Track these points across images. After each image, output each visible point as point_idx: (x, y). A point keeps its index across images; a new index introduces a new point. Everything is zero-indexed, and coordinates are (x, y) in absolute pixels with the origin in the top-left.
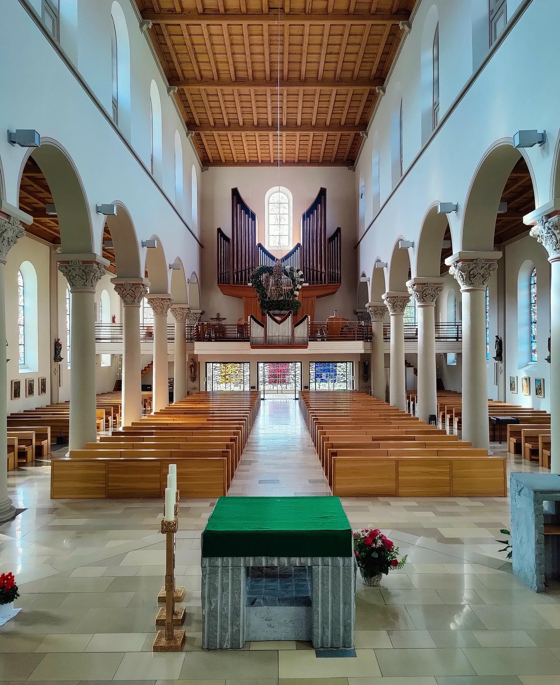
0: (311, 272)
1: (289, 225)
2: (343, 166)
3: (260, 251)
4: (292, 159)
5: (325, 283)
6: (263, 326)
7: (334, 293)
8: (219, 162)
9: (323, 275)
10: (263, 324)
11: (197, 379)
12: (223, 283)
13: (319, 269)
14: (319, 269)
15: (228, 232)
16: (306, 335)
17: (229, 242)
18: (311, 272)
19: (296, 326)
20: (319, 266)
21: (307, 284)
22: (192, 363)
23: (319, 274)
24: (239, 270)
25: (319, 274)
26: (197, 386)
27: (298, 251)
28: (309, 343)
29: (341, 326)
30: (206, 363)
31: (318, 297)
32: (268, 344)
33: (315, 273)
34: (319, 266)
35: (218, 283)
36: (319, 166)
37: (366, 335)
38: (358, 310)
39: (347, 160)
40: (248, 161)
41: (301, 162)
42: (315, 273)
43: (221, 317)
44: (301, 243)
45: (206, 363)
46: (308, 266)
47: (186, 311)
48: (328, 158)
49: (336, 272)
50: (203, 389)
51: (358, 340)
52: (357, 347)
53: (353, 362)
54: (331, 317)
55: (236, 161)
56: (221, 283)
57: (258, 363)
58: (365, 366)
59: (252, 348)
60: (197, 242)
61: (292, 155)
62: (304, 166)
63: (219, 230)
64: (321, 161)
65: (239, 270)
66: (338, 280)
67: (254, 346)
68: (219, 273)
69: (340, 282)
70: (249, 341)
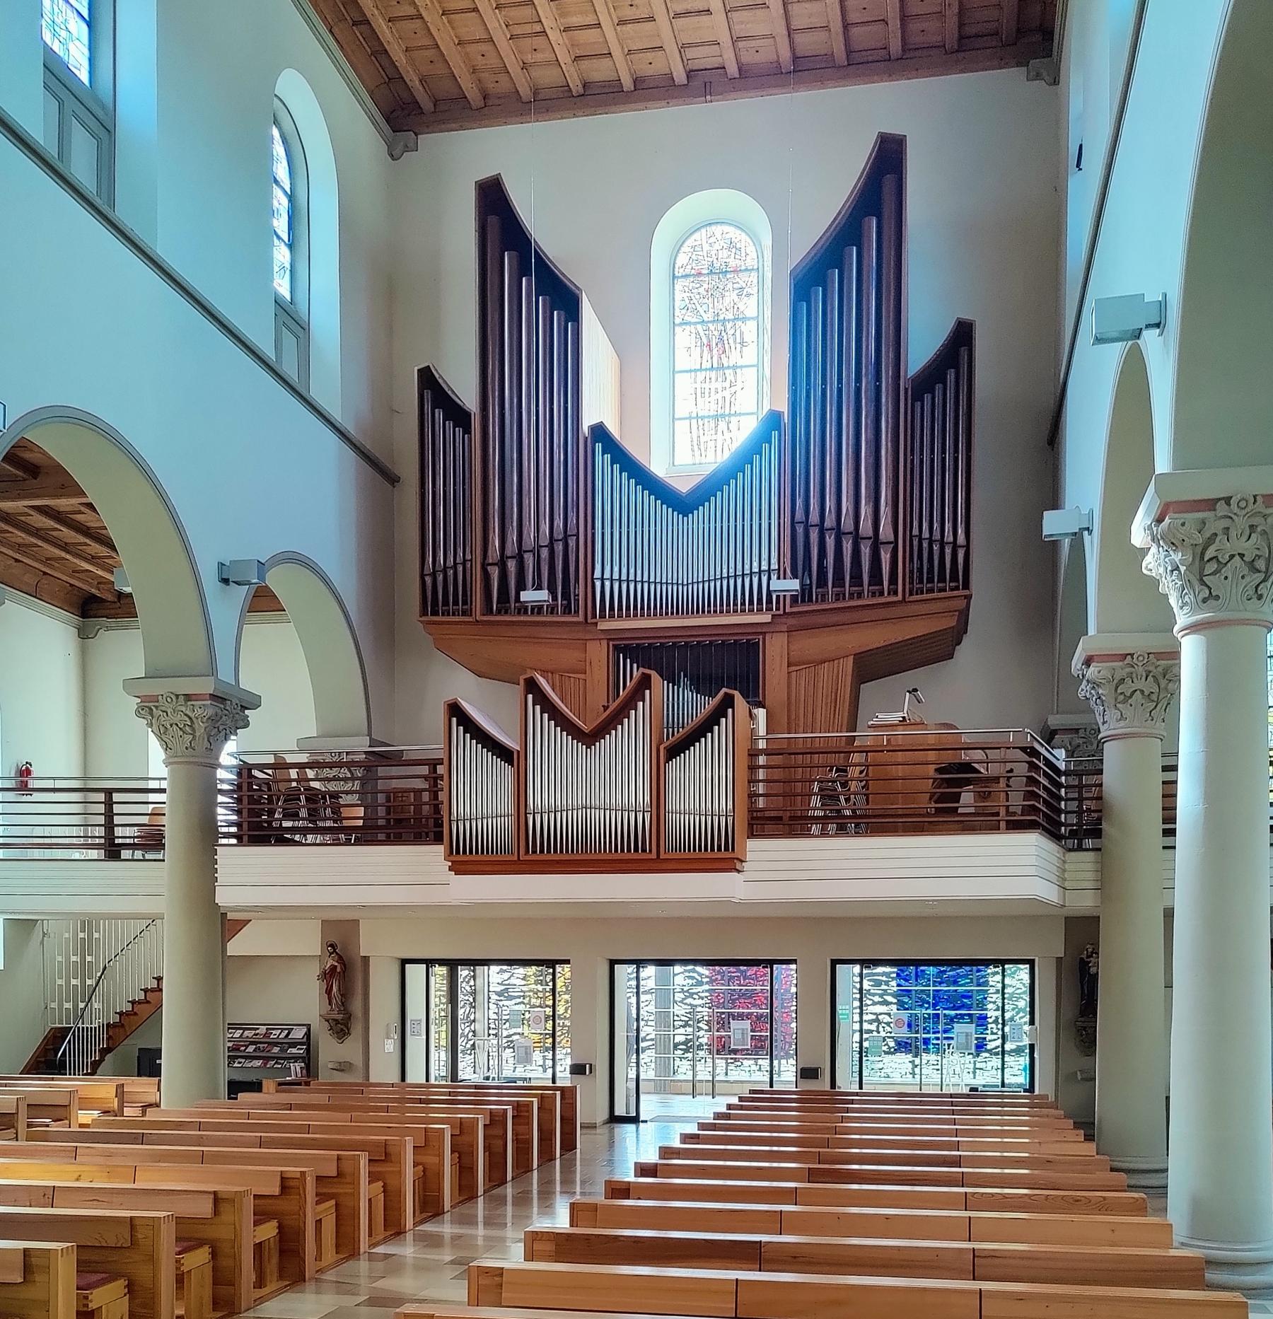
0: (830, 542)
1: (758, 366)
3: (602, 460)
6: (504, 753)
9: (885, 557)
11: (357, 1029)
13: (866, 527)
14: (866, 527)
16: (723, 803)
17: (467, 430)
18: (830, 542)
19: (676, 750)
20: (865, 510)
22: (330, 962)
23: (866, 551)
24: (511, 548)
25: (866, 551)
26: (358, 1061)
32: (534, 852)
33: (847, 546)
34: (865, 510)
37: (1068, 809)
38: (1054, 721)
42: (847, 546)
45: (404, 962)
46: (814, 517)
47: (203, 710)
49: (949, 537)
50: (383, 1070)
51: (1016, 826)
57: (613, 963)
59: (459, 868)
60: (332, 437)
63: (428, 379)
65: (511, 548)
66: (954, 577)
67: (468, 860)
69: (966, 585)
70: (438, 839)
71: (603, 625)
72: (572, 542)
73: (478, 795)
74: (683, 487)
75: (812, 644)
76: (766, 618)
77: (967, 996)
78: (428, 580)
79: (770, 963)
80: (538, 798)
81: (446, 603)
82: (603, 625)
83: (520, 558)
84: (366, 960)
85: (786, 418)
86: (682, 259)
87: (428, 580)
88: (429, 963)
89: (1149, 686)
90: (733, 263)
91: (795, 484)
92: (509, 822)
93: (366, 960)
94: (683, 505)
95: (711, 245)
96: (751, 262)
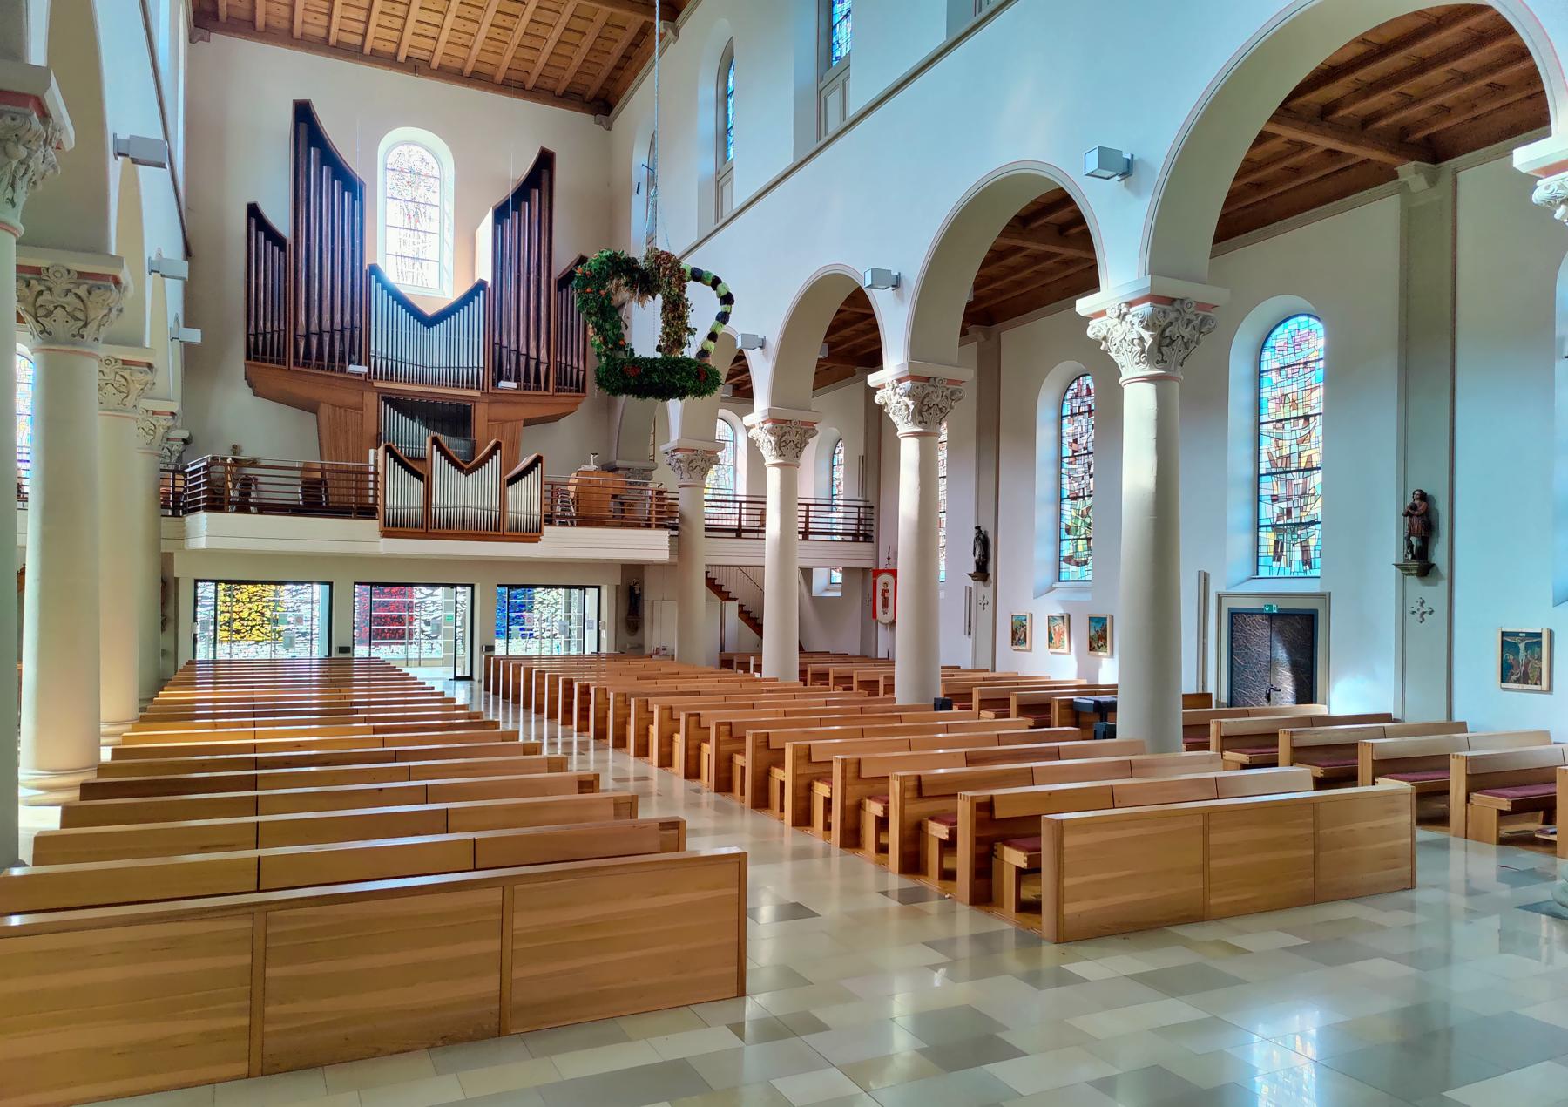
2: (583, 111)
4: (457, 64)
5: (546, 388)
7: (555, 418)
8: (246, 26)
9: (543, 368)
10: (414, 467)
11: (170, 627)
12: (264, 361)
13: (533, 353)
14: (533, 353)
15: (281, 221)
20: (533, 344)
21: (513, 385)
24: (314, 327)
25: (532, 363)
27: (479, 300)
28: (546, 529)
29: (611, 491)
30: (197, 581)
31: (528, 423)
32: (430, 526)
33: (523, 359)
34: (533, 344)
35: (248, 358)
36: (525, 97)
39: (596, 99)
40: (332, 40)
41: (477, 78)
42: (523, 359)
43: (247, 454)
44: (488, 278)
48: (550, 84)
51: (658, 526)
52: (651, 545)
53: (599, 588)
54: (585, 467)
55: (297, 33)
56: (256, 359)
58: (632, 594)
59: (386, 534)
61: (461, 52)
62: (486, 89)
64: (529, 85)
65: (314, 327)
67: (393, 529)
68: (252, 331)
71: (377, 384)
72: (357, 332)
73: (402, 493)
74: (430, 310)
75: (500, 411)
76: (477, 394)
77: (522, 605)
78: (252, 339)
79: (455, 585)
80: (437, 500)
81: (264, 353)
82: (377, 384)
83: (320, 334)
84: (177, 580)
85: (490, 284)
86: (391, 159)
87: (252, 339)
88: (217, 582)
89: (702, 465)
90: (424, 171)
91: (494, 322)
92: (420, 511)
93: (177, 580)
94: (430, 322)
95: (413, 156)
96: (436, 173)
